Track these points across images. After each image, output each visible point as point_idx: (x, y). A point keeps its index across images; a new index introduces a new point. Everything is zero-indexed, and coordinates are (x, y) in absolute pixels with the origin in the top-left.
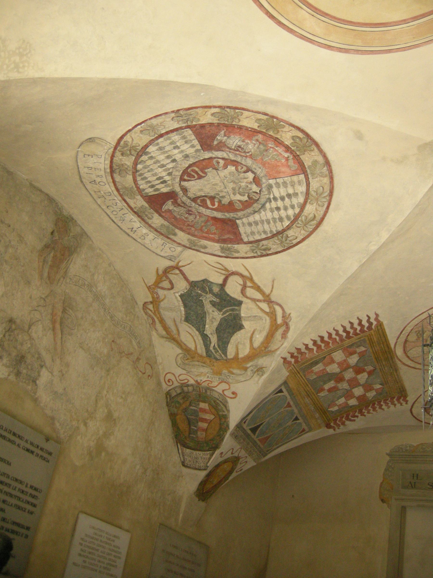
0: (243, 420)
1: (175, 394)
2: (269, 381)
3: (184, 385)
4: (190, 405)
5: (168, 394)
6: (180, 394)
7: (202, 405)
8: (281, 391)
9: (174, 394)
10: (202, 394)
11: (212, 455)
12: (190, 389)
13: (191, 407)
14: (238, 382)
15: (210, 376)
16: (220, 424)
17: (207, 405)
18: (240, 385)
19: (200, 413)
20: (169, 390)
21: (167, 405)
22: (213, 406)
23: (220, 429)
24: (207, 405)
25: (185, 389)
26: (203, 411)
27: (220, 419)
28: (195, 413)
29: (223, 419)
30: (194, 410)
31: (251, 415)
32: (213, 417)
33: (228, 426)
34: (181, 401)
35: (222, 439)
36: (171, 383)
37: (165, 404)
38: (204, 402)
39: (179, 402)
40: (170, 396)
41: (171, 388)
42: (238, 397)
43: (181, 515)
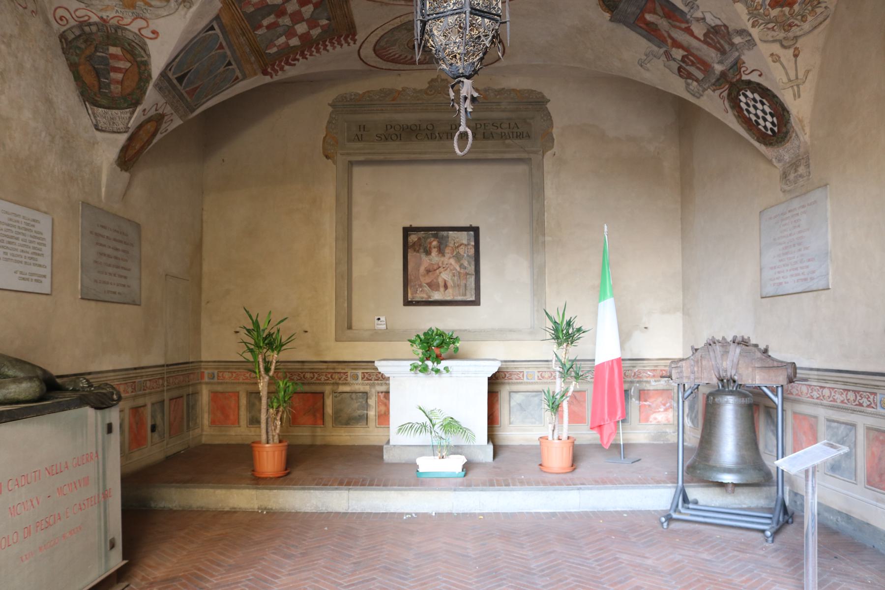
0: (169, 66)
1: (73, 36)
2: (199, 15)
3: (83, 24)
4: (96, 50)
5: (62, 37)
6: (80, 36)
7: (113, 50)
8: (212, 28)
9: (71, 37)
10: (112, 34)
11: (133, 113)
12: (94, 29)
13: (98, 54)
14: (159, 17)
15: (119, 10)
16: (140, 73)
17: (119, 49)
18: (161, 21)
19: (111, 61)
20: (64, 32)
21: (64, 53)
22: (128, 51)
23: (140, 79)
24: (119, 49)
25: (87, 29)
26: (115, 57)
27: (139, 67)
28: (104, 61)
29: (142, 66)
30: (102, 57)
31: (177, 60)
32: (129, 65)
33: (150, 76)
34: (83, 46)
35: (144, 93)
36: (65, 22)
37: (60, 52)
38: (115, 45)
39: (79, 48)
40: (66, 40)
41: (65, 28)
42: (159, 38)
43: (103, 190)
